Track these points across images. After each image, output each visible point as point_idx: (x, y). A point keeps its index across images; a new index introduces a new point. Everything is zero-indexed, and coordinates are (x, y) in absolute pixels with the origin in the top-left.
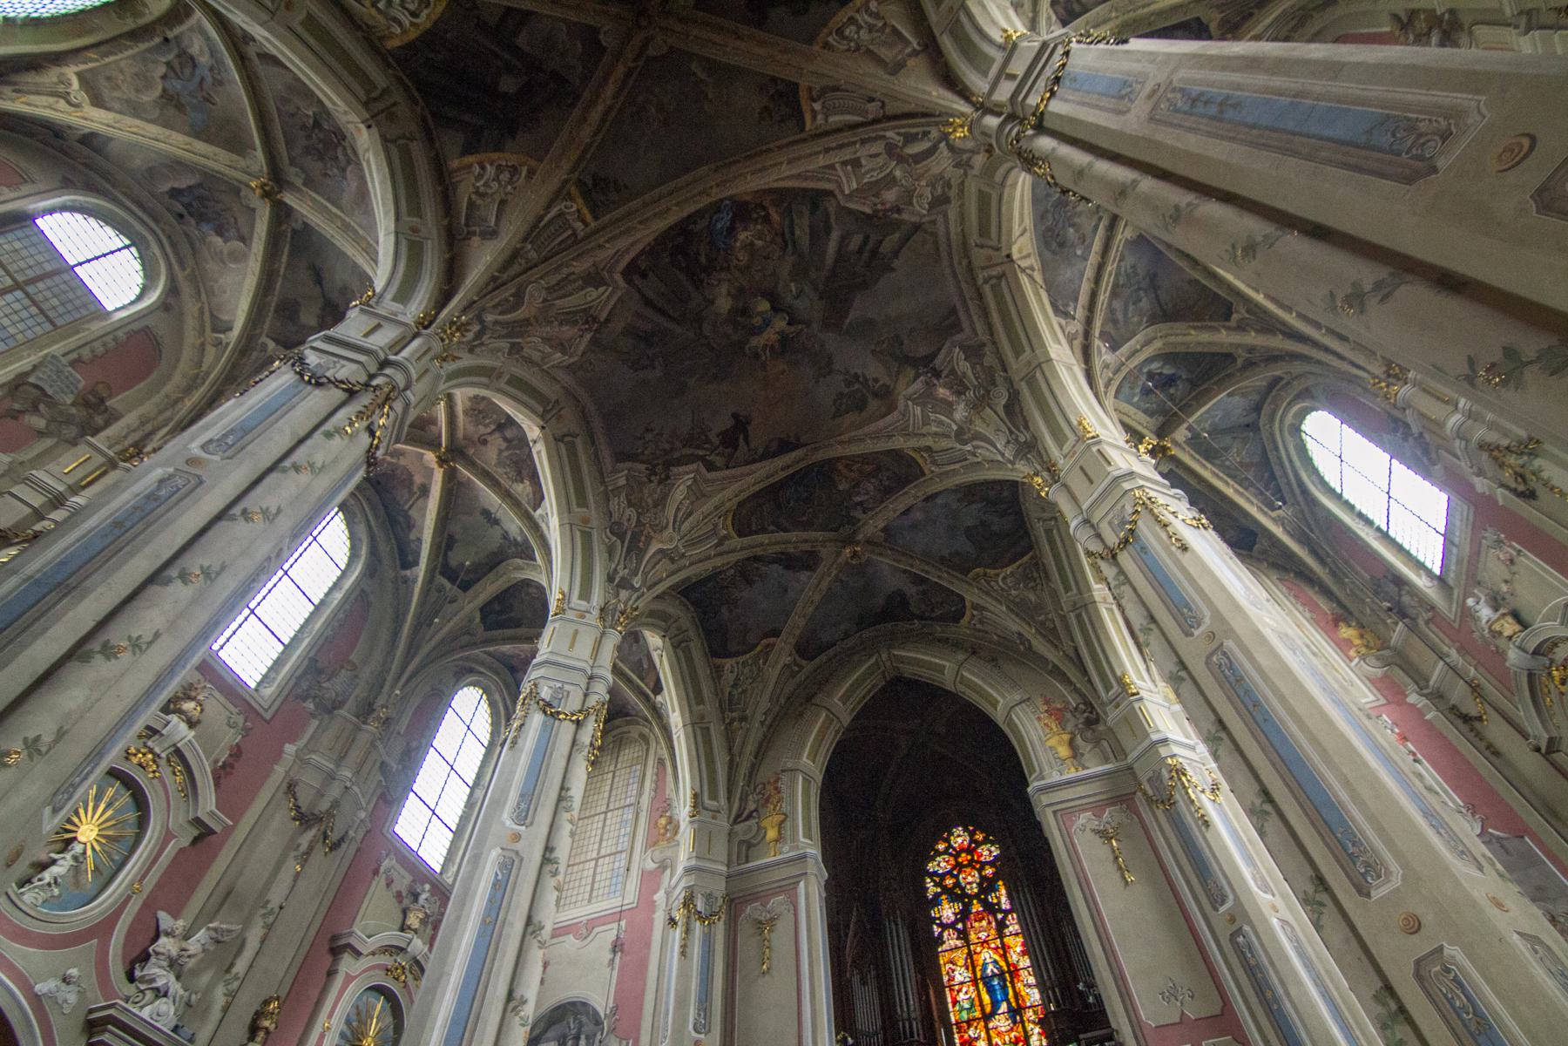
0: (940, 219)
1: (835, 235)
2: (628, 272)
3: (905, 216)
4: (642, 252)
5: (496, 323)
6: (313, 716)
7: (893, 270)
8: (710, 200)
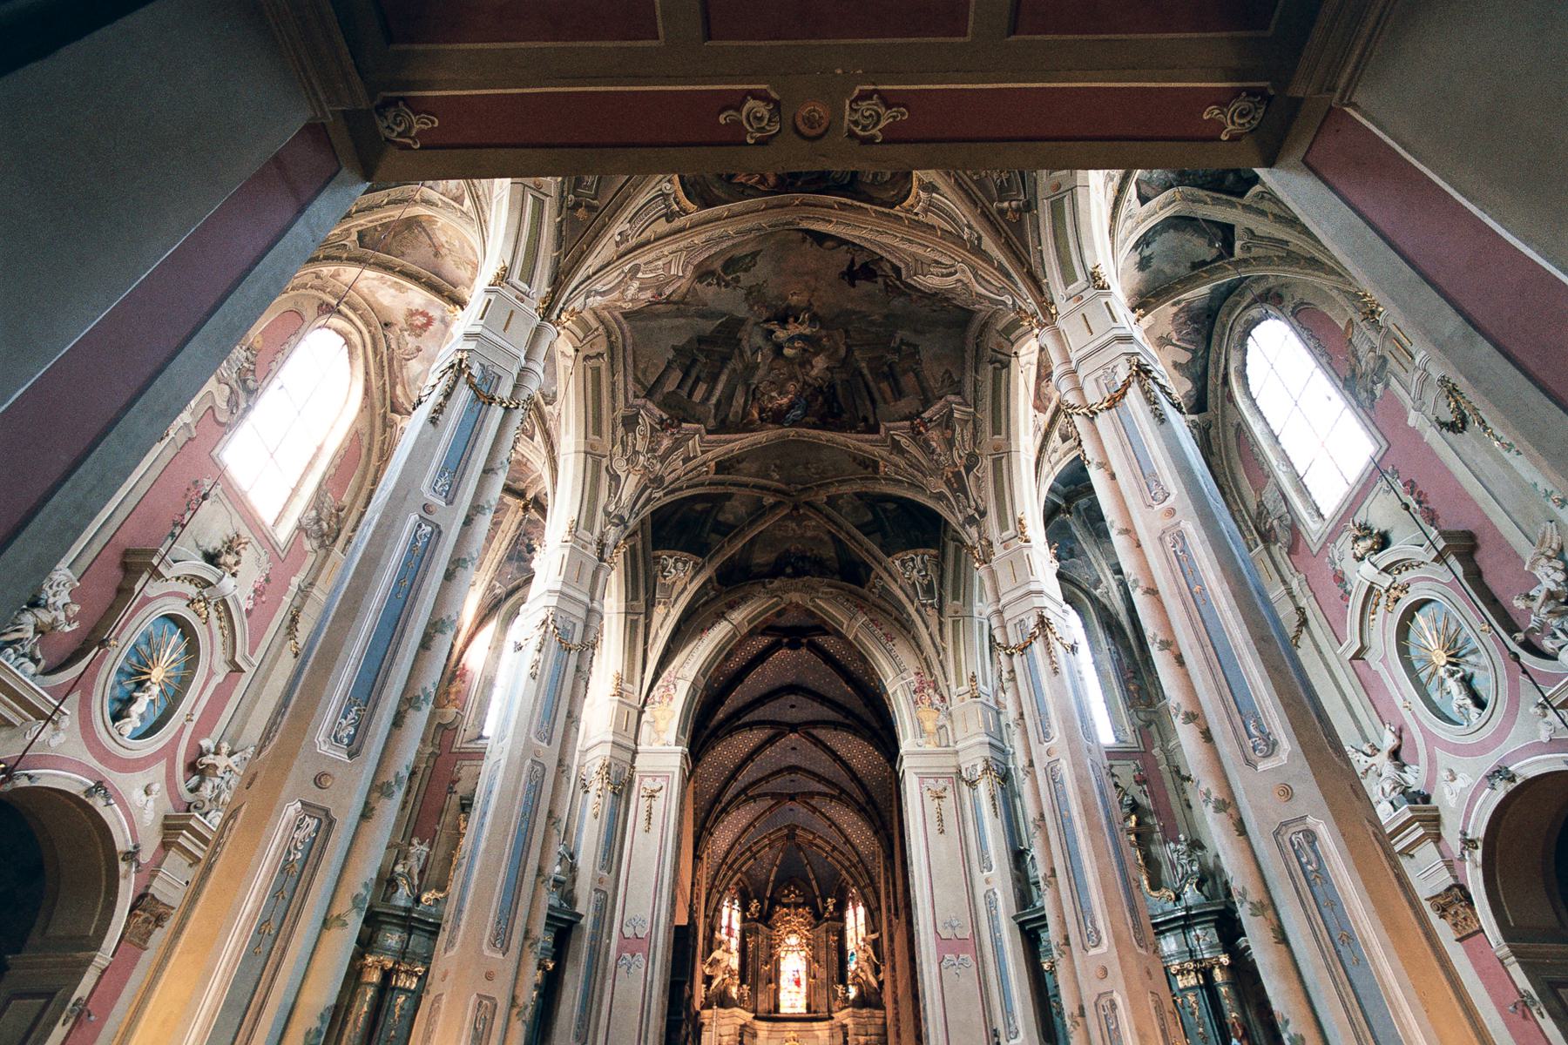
0: (631, 400)
1: (714, 400)
2: (874, 429)
3: (657, 412)
6: (1387, 386)
7: (674, 347)
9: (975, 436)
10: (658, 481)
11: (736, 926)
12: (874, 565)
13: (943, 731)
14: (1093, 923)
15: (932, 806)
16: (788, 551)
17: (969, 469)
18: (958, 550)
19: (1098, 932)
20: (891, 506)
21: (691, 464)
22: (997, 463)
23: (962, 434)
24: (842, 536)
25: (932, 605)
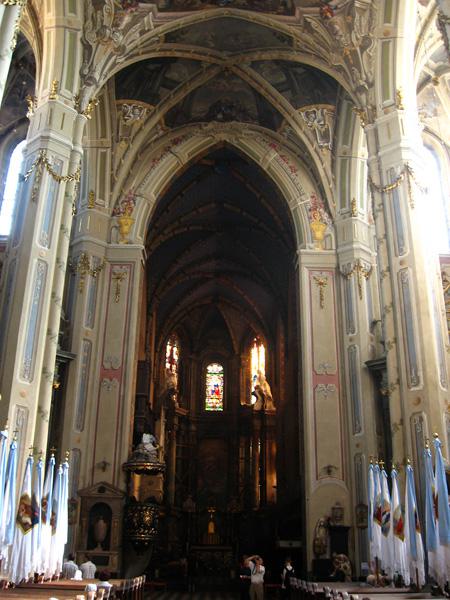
2: (291, 12)
4: (278, 14)
5: (354, 82)
8: (229, 9)
9: (370, 23)
10: (121, 49)
11: (176, 357)
12: (286, 115)
13: (328, 239)
14: (416, 372)
15: (316, 290)
16: (219, 101)
17: (363, 49)
18: (349, 106)
19: (418, 378)
20: (300, 70)
21: (146, 36)
22: (385, 46)
23: (361, 21)
24: (262, 92)
25: (327, 147)
